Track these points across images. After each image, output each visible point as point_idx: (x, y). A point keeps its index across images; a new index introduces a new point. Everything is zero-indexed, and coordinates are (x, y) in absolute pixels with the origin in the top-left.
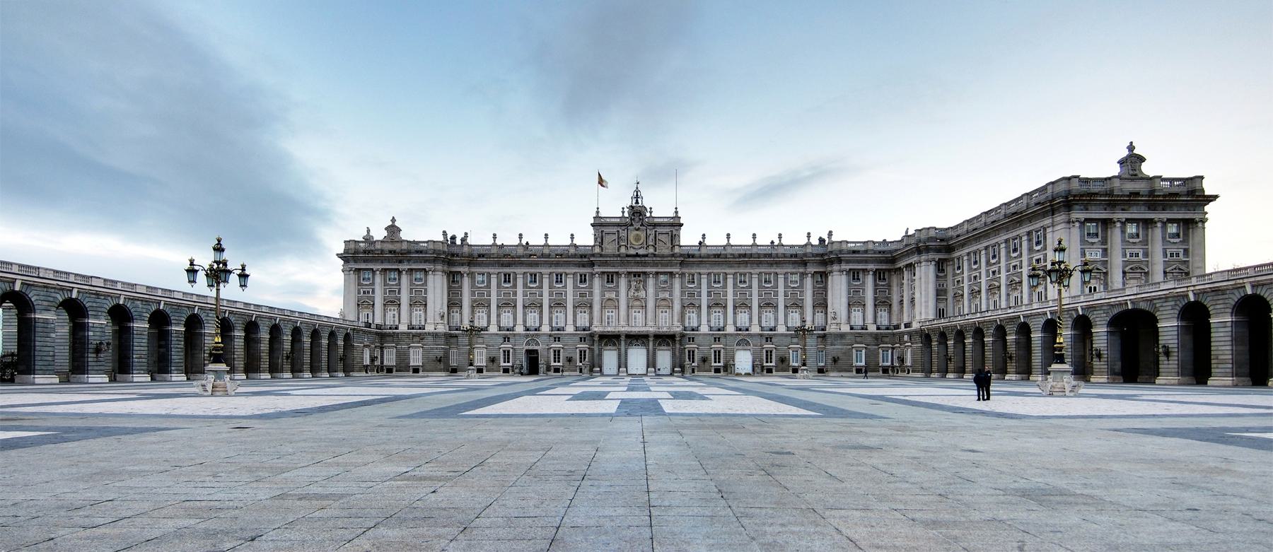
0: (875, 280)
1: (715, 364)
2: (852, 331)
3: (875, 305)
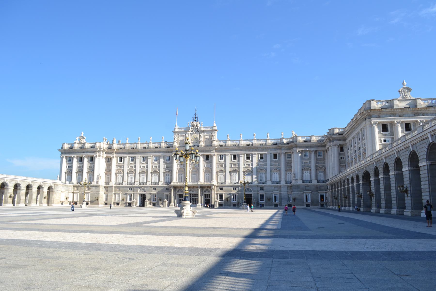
0: (316, 156)
1: (233, 202)
2: (303, 184)
3: (317, 170)
